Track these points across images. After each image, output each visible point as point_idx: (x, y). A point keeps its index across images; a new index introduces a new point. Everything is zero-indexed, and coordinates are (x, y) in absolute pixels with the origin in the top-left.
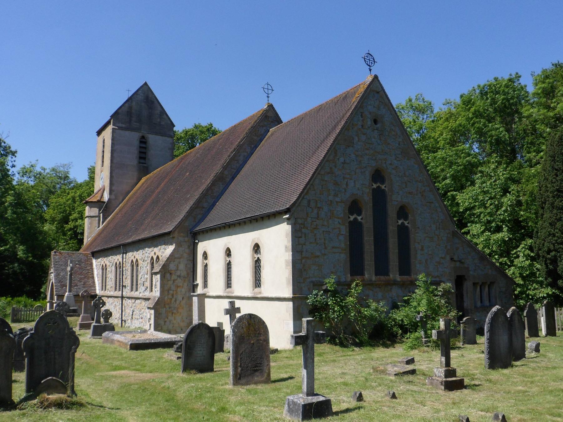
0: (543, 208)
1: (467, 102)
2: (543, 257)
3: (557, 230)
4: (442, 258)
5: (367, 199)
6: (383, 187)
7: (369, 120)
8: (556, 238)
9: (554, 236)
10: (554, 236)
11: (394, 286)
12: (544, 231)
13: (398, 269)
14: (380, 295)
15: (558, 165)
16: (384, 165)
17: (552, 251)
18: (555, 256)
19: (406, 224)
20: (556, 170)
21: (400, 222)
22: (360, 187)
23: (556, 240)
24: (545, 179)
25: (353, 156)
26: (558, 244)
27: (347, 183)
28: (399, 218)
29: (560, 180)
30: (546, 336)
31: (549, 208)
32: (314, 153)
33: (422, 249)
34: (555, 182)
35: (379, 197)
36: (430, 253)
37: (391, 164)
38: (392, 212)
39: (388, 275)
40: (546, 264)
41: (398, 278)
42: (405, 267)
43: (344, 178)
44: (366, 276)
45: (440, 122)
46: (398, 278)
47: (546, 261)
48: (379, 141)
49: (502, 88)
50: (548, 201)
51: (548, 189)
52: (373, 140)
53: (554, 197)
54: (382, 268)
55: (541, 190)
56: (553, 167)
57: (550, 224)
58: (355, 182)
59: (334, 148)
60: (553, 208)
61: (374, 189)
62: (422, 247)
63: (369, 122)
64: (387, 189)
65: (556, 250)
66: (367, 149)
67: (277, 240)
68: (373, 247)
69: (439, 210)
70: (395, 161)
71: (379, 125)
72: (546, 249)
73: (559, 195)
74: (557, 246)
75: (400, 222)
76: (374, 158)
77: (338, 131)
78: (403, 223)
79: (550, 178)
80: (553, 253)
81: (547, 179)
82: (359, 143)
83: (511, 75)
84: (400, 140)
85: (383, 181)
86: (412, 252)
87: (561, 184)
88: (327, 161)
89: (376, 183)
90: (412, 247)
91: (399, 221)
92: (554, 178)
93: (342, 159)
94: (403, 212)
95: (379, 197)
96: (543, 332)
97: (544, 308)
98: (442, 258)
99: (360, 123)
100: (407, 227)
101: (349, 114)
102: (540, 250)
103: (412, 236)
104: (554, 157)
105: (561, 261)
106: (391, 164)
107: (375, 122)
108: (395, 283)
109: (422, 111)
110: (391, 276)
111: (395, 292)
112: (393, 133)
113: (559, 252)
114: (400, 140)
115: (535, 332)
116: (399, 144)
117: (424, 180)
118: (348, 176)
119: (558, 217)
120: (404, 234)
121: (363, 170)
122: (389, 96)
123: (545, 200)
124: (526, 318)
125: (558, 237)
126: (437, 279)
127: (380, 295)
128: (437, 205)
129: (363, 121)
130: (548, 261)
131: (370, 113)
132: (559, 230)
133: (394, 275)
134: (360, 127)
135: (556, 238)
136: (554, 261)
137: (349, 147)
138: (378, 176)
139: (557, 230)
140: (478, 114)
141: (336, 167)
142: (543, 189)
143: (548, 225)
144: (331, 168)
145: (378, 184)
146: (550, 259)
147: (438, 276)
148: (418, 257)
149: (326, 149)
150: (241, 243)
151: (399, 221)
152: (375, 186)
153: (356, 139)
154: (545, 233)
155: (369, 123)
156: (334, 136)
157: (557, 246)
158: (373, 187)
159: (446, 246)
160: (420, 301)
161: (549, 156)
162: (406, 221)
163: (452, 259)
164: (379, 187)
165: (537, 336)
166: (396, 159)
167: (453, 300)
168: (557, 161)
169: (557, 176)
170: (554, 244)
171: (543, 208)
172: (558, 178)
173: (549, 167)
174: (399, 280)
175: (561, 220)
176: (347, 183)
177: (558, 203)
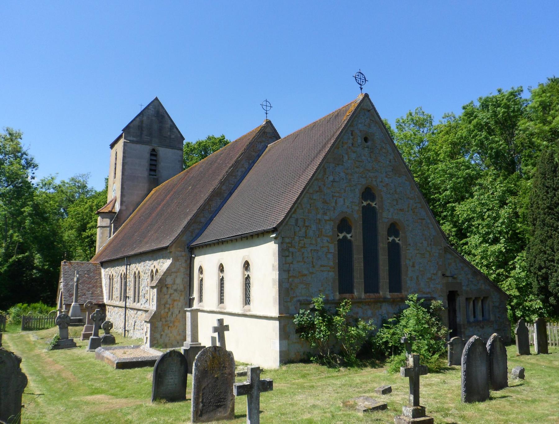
0: (534, 225)
1: (470, 115)
2: (535, 273)
3: (548, 248)
4: (434, 274)
5: (356, 217)
6: (373, 205)
7: (359, 138)
8: (546, 256)
9: (545, 253)
10: (545, 253)
11: (384, 304)
12: (535, 248)
13: (388, 286)
14: (369, 312)
15: (548, 182)
16: (375, 183)
17: (543, 269)
18: (546, 273)
19: (397, 241)
20: (547, 187)
21: (391, 239)
22: (350, 205)
23: (547, 258)
24: (536, 196)
25: (342, 175)
26: (549, 261)
27: (336, 200)
28: (389, 235)
29: (551, 197)
30: (538, 353)
31: (540, 225)
32: (304, 171)
33: (413, 266)
34: (546, 200)
35: (369, 216)
36: (421, 269)
37: (381, 182)
38: (382, 230)
39: (378, 292)
40: (537, 280)
41: (388, 295)
42: (396, 284)
43: (333, 196)
44: (356, 294)
45: (441, 135)
46: (388, 295)
47: (537, 278)
48: (369, 159)
49: (505, 101)
50: (539, 218)
51: (540, 206)
52: (363, 158)
53: (545, 214)
54: (371, 285)
55: (532, 207)
56: (543, 184)
57: (541, 241)
58: (344, 200)
59: (323, 167)
60: (544, 225)
61: (364, 207)
62: (414, 263)
63: (359, 140)
64: (377, 206)
65: (545, 267)
66: (357, 167)
67: (265, 258)
68: (363, 264)
69: (431, 226)
70: (386, 179)
71: (369, 143)
72: (537, 266)
73: (550, 213)
74: (548, 264)
75: (391, 239)
76: (364, 176)
77: (327, 150)
78: (393, 240)
79: (541, 196)
80: (544, 271)
81: (539, 196)
82: (349, 161)
83: (513, 88)
84: (391, 158)
85: (373, 199)
86: (403, 269)
87: (552, 201)
88: (317, 179)
89: (366, 200)
90: (403, 263)
91: (389, 238)
92: (545, 195)
93: (331, 178)
94: (393, 229)
95: (369, 216)
96: (534, 349)
97: (535, 324)
98: (434, 274)
99: (350, 141)
100: (398, 244)
101: (338, 133)
102: (532, 266)
103: (403, 253)
104: (545, 175)
105: (552, 279)
106: (381, 182)
107: (366, 140)
108: (385, 300)
109: (420, 124)
110: (381, 293)
111: (385, 309)
112: (384, 150)
113: (550, 269)
114: (391, 158)
115: (525, 350)
116: (390, 162)
117: (416, 196)
118: (337, 195)
119: (549, 234)
120: (394, 251)
121: (352, 188)
122: (380, 114)
123: (536, 217)
124: (516, 336)
125: (548, 254)
126: (429, 296)
127: (369, 312)
128: (429, 221)
129: (353, 139)
130: (540, 278)
131: (361, 131)
132: (550, 247)
133: (384, 292)
134: (351, 145)
135: (546, 256)
136: (545, 278)
137: (338, 165)
138: (368, 193)
139: (548, 248)
140: (480, 127)
141: (325, 185)
142: (535, 205)
143: (539, 242)
144: (320, 187)
145: (369, 202)
146: (541, 276)
147: (429, 293)
148: (409, 276)
149: (315, 168)
150: (232, 258)
151: (389, 238)
152: (365, 204)
153: (346, 157)
154: (537, 250)
155: (359, 141)
156: (324, 154)
157: (548, 264)
158: (363, 205)
159: (438, 264)
160: (411, 319)
161: (540, 173)
162: (396, 238)
163: (443, 275)
164: (369, 204)
165: (528, 353)
166: (386, 177)
167: (445, 316)
168: (548, 179)
169: (548, 193)
170: (545, 262)
171: (534, 225)
172: (549, 195)
173: (540, 184)
174: (389, 297)
175: (551, 237)
176: (336, 200)
177: (548, 220)
